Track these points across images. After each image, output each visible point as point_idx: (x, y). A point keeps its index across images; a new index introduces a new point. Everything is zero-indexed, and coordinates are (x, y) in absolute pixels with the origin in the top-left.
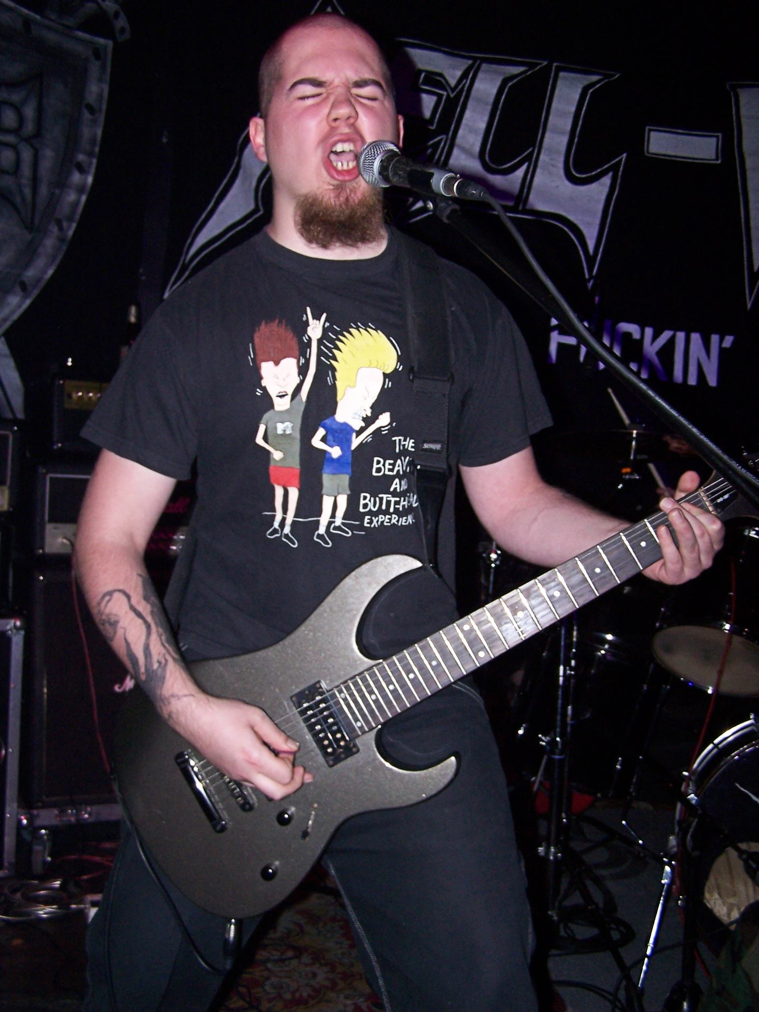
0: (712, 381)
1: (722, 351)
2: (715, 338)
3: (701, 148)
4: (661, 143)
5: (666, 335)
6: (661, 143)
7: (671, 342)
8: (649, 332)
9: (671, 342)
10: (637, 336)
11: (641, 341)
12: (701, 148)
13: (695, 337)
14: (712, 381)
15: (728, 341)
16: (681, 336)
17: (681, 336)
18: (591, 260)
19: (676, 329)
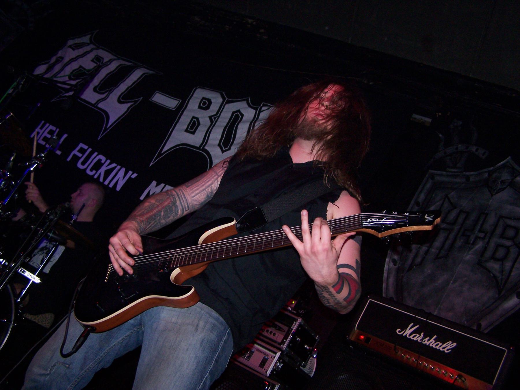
0: (118, 188)
1: (130, 177)
2: (130, 172)
3: (171, 103)
4: (159, 98)
5: (114, 165)
6: (159, 98)
7: (113, 169)
8: (108, 161)
9: (113, 169)
10: (103, 162)
11: (103, 164)
12: (171, 103)
13: (123, 170)
14: (118, 188)
15: (135, 175)
17: (119, 167)
18: (106, 129)
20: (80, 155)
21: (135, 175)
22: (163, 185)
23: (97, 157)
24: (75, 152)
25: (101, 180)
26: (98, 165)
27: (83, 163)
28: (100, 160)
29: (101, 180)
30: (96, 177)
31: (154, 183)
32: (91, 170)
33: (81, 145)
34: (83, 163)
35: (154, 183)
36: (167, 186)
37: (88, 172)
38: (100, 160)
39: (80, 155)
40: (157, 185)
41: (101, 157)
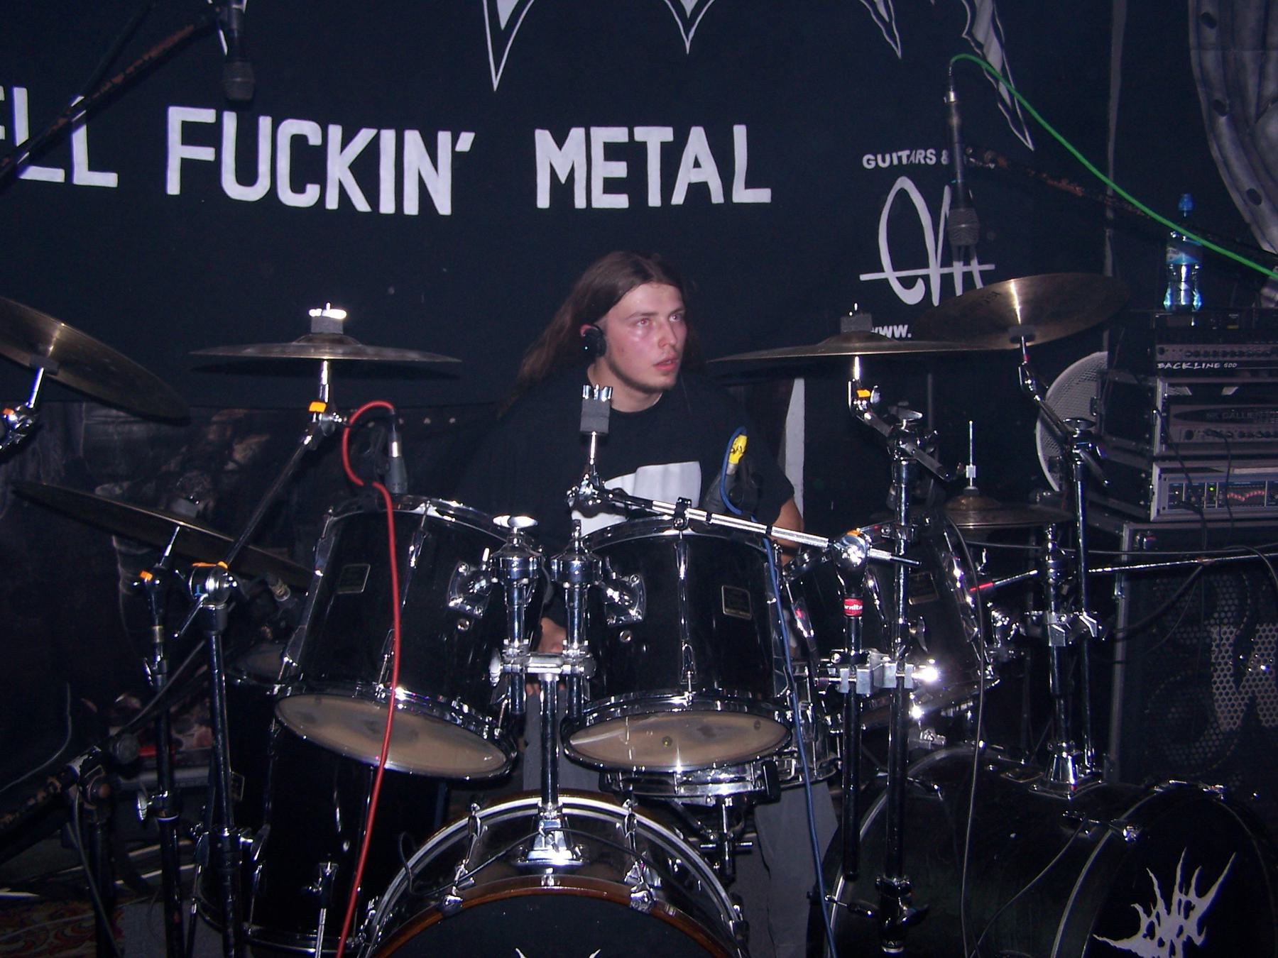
0: (444, 205)
1: (456, 157)
2: (444, 138)
5: (364, 137)
7: (373, 150)
8: (335, 132)
9: (373, 150)
10: (315, 139)
11: (323, 149)
13: (413, 138)
14: (444, 205)
15: (466, 141)
16: (388, 137)
17: (388, 137)
19: (380, 126)
20: (206, 154)
21: (466, 141)
22: (577, 134)
23: (279, 137)
24: (177, 152)
25: (361, 204)
26: (309, 164)
27: (247, 175)
28: (298, 142)
29: (361, 204)
30: (332, 203)
31: (543, 138)
32: (298, 187)
33: (177, 116)
34: (247, 175)
35: (543, 138)
36: (594, 130)
37: (288, 197)
38: (298, 142)
39: (206, 154)
40: (560, 141)
41: (291, 127)
